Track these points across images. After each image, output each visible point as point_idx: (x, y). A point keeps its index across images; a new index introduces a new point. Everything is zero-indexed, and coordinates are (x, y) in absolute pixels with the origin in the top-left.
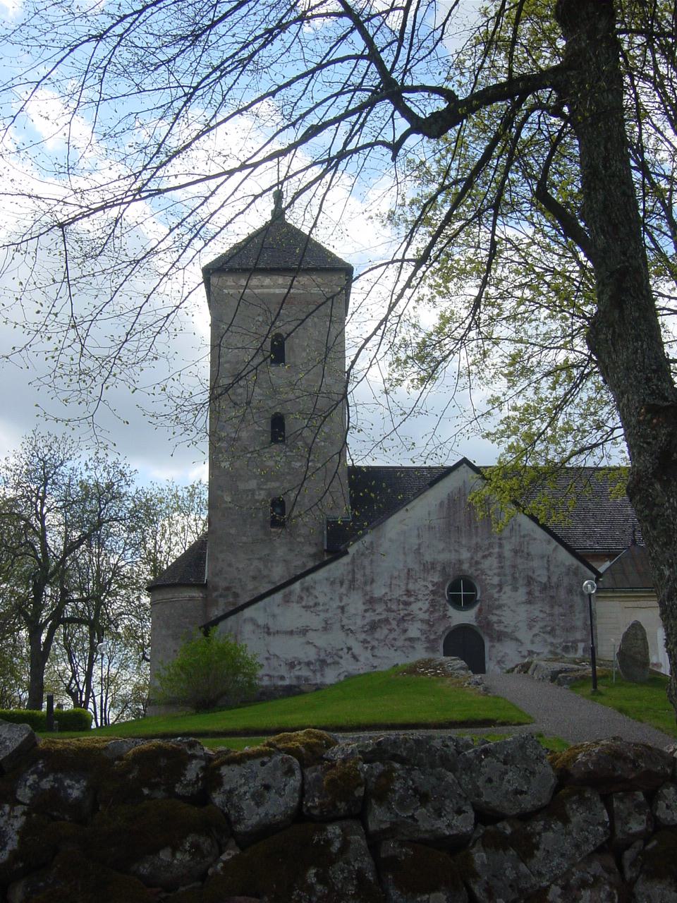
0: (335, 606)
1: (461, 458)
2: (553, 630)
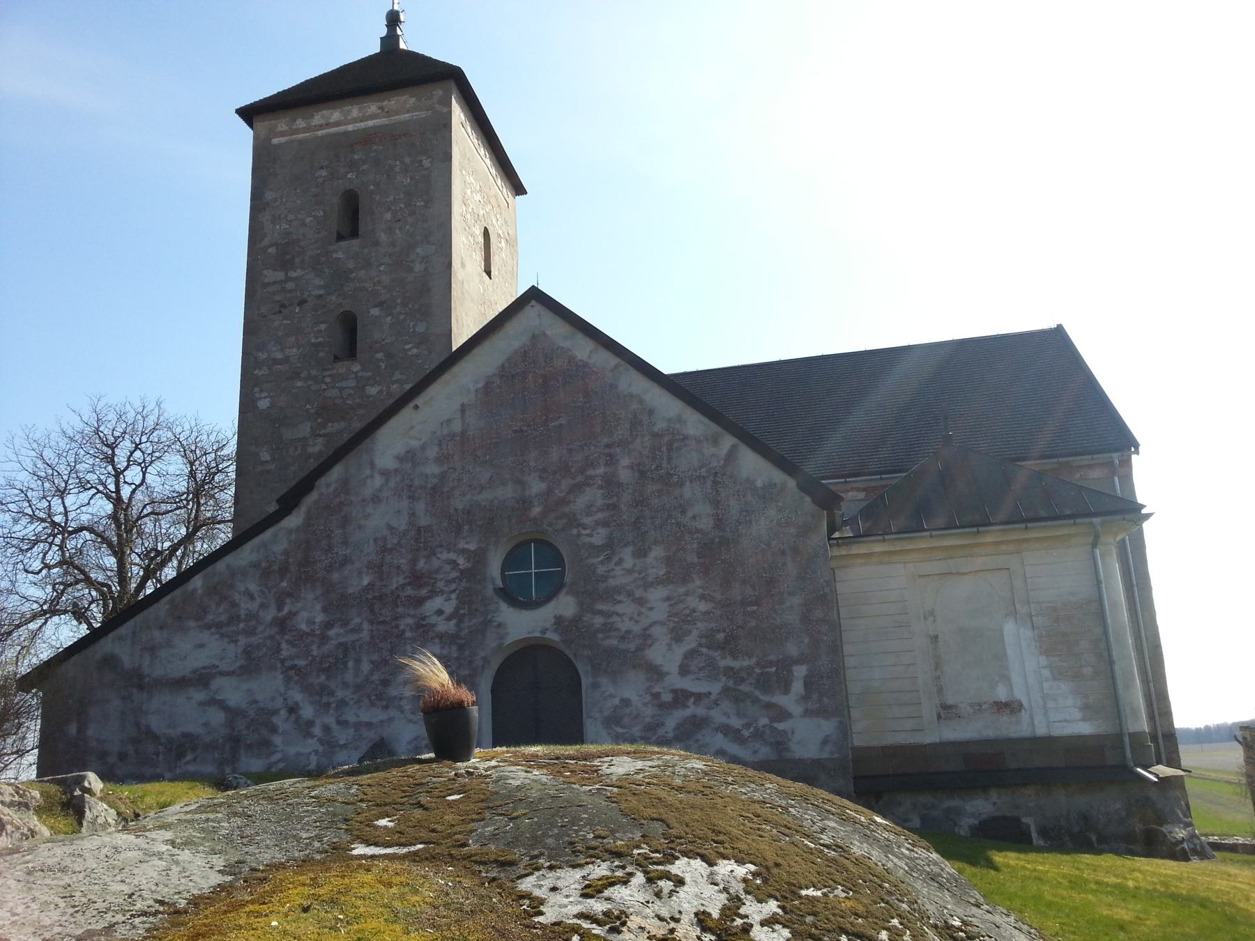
0: (269, 618)
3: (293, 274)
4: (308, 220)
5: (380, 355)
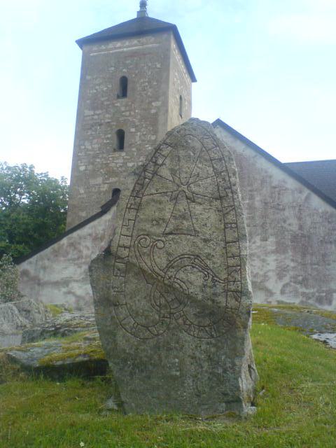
3: (98, 112)
5: (134, 149)
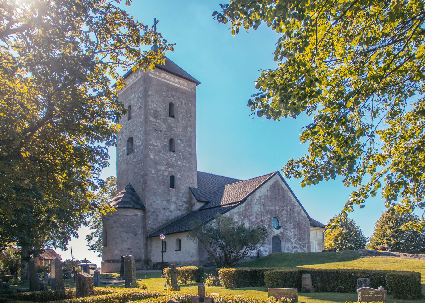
1: (274, 171)
2: (300, 239)
3: (157, 121)
4: (161, 106)
